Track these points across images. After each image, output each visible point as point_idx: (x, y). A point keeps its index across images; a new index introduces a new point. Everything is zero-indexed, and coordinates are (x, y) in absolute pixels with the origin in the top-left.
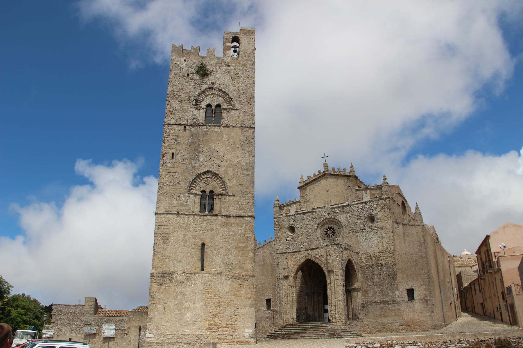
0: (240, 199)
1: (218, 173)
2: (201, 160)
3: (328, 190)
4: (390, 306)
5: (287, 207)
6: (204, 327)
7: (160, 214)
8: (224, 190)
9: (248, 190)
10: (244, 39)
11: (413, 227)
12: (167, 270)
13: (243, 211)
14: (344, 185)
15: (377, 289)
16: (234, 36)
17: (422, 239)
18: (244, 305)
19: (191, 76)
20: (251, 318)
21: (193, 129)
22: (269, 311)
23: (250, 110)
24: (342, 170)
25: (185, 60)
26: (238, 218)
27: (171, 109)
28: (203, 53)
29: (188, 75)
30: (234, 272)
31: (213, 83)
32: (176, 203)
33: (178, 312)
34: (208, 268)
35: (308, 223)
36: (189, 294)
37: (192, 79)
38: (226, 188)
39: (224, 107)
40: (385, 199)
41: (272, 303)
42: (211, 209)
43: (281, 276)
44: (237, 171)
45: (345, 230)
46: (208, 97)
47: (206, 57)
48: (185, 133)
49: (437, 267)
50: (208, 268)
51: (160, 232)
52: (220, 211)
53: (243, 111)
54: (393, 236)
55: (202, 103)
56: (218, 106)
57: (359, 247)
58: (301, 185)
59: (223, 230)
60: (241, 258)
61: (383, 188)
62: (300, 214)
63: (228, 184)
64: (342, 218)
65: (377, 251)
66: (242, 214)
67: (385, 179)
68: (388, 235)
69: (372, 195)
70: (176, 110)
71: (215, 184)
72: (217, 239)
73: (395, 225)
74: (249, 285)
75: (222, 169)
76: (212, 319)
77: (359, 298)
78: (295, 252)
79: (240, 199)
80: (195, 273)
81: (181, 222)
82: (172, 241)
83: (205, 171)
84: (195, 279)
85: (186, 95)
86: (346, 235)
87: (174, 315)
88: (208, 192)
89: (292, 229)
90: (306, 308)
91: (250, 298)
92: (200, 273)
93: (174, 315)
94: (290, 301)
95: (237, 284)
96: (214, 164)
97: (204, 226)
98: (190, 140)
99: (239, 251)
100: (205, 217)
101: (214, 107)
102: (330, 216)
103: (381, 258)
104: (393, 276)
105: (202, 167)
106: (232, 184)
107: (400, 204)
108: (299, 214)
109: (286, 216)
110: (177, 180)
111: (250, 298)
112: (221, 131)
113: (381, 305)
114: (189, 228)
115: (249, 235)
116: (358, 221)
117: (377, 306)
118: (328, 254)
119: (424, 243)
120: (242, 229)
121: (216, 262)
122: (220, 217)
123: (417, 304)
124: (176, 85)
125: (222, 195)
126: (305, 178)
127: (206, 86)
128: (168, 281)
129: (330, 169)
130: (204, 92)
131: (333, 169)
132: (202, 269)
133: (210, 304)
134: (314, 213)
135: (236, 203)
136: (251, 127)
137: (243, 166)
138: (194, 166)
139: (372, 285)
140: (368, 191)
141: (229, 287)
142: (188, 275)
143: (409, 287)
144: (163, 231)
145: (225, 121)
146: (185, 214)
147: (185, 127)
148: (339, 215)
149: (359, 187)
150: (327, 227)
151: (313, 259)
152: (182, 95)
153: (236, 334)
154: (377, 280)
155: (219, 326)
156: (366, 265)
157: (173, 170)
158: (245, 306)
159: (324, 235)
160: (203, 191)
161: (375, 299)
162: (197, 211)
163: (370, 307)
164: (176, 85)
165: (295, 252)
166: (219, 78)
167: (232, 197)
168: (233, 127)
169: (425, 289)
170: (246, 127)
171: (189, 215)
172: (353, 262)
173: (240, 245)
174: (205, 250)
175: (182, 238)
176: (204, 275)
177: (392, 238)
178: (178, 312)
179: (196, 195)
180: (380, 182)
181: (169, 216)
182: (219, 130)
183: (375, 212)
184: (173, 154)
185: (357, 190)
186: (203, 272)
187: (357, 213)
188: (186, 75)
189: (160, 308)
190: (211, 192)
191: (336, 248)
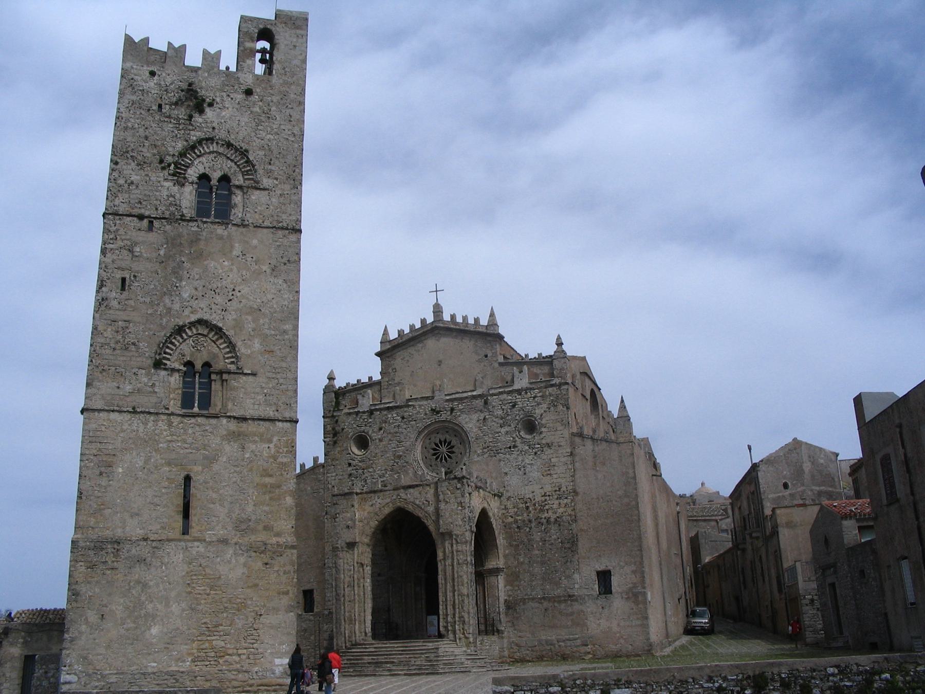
0: (267, 383)
1: (220, 325)
2: (185, 295)
3: (440, 362)
4: (563, 606)
5: (353, 394)
6: (189, 654)
7: (94, 410)
8: (232, 363)
9: (284, 365)
10: (283, 36)
11: (614, 446)
12: (108, 533)
13: (274, 408)
14: (477, 353)
15: (537, 569)
16: (261, 26)
17: (631, 471)
18: (274, 608)
19: (166, 108)
20: (289, 634)
21: (168, 227)
22: (309, 616)
23: (293, 191)
24: (471, 321)
25: (153, 74)
26: (262, 423)
27: (121, 181)
28: (193, 59)
29: (160, 106)
30: (253, 538)
31: (214, 128)
32: (128, 388)
33: (132, 625)
34: (198, 528)
35: (396, 430)
36: (157, 585)
37: (169, 117)
38: (237, 357)
39: (237, 183)
40: (560, 385)
41: (317, 597)
42: (206, 402)
43: (341, 543)
44: (261, 321)
45: (474, 447)
46: (203, 159)
47: (199, 68)
48: (150, 235)
49: (657, 525)
50: (198, 528)
51: (95, 452)
52: (224, 405)
53: (278, 192)
54: (573, 462)
55: (190, 171)
56: (225, 179)
57: (503, 482)
58: (385, 348)
59: (230, 449)
60: (266, 508)
61: (555, 362)
62: (380, 410)
63: (242, 350)
64: (470, 422)
65: (538, 494)
66: (272, 414)
67: (559, 344)
68: (563, 459)
69: (533, 375)
70: (132, 183)
71: (215, 350)
72: (216, 467)
73: (577, 440)
74: (284, 565)
75: (231, 317)
76: (204, 638)
77: (501, 587)
78: (371, 492)
79: (267, 383)
80: (169, 540)
81: (141, 430)
82: (120, 470)
83: (193, 319)
84: (169, 553)
85: (155, 151)
86: (476, 458)
87: (122, 632)
88: (198, 366)
89: (363, 442)
90: (389, 610)
91: (287, 593)
92: (180, 540)
93: (122, 632)
94: (359, 596)
95: (260, 564)
96: (213, 306)
97: (190, 440)
98: (162, 252)
99: (264, 493)
100: (193, 420)
101: (214, 182)
103: (547, 507)
104: (571, 545)
105: (187, 312)
106: (250, 349)
107: (588, 397)
108: (376, 410)
109: (350, 414)
110: (131, 338)
111: (287, 593)
112: (229, 236)
113: (546, 604)
114: (158, 442)
115: (285, 460)
116: (503, 430)
117: (537, 605)
118: (441, 497)
119: (635, 478)
120: (272, 446)
121: (214, 516)
122: (224, 421)
123: (618, 603)
124: (133, 128)
125: (229, 373)
126: (393, 335)
127: (198, 134)
128: (110, 558)
129: (447, 317)
130: (193, 148)
131: (453, 317)
132: (185, 531)
133: (200, 607)
135: (258, 390)
136: (293, 229)
137: (275, 312)
138: (170, 309)
139: (527, 561)
140: (525, 368)
141: (240, 571)
142: (154, 544)
143: (601, 568)
144: (100, 450)
145: (237, 214)
146: (149, 413)
147: (151, 223)
148: (464, 416)
149: (505, 358)
150: (436, 438)
151: (410, 508)
152: (145, 150)
153: (256, 669)
154: (537, 552)
155: (221, 654)
156: (516, 521)
157: (122, 315)
158: (276, 610)
159: (429, 456)
160: (189, 364)
161: (532, 590)
162: (175, 405)
163: (523, 607)
164: (133, 128)
165: (371, 492)
166: (225, 117)
167: (251, 378)
168: (256, 227)
169: (634, 572)
170: (282, 228)
171: (157, 414)
172: (491, 514)
173: (267, 480)
174: (193, 491)
175: (141, 464)
176: (190, 544)
177: (570, 467)
178: (132, 625)
179: (173, 370)
180: (549, 350)
181: (114, 416)
182: (226, 233)
183: (538, 411)
184: (124, 280)
185: (501, 364)
186: (186, 537)
187: (500, 412)
188: (155, 108)
189: (93, 617)
190: (207, 365)
191: (459, 486)
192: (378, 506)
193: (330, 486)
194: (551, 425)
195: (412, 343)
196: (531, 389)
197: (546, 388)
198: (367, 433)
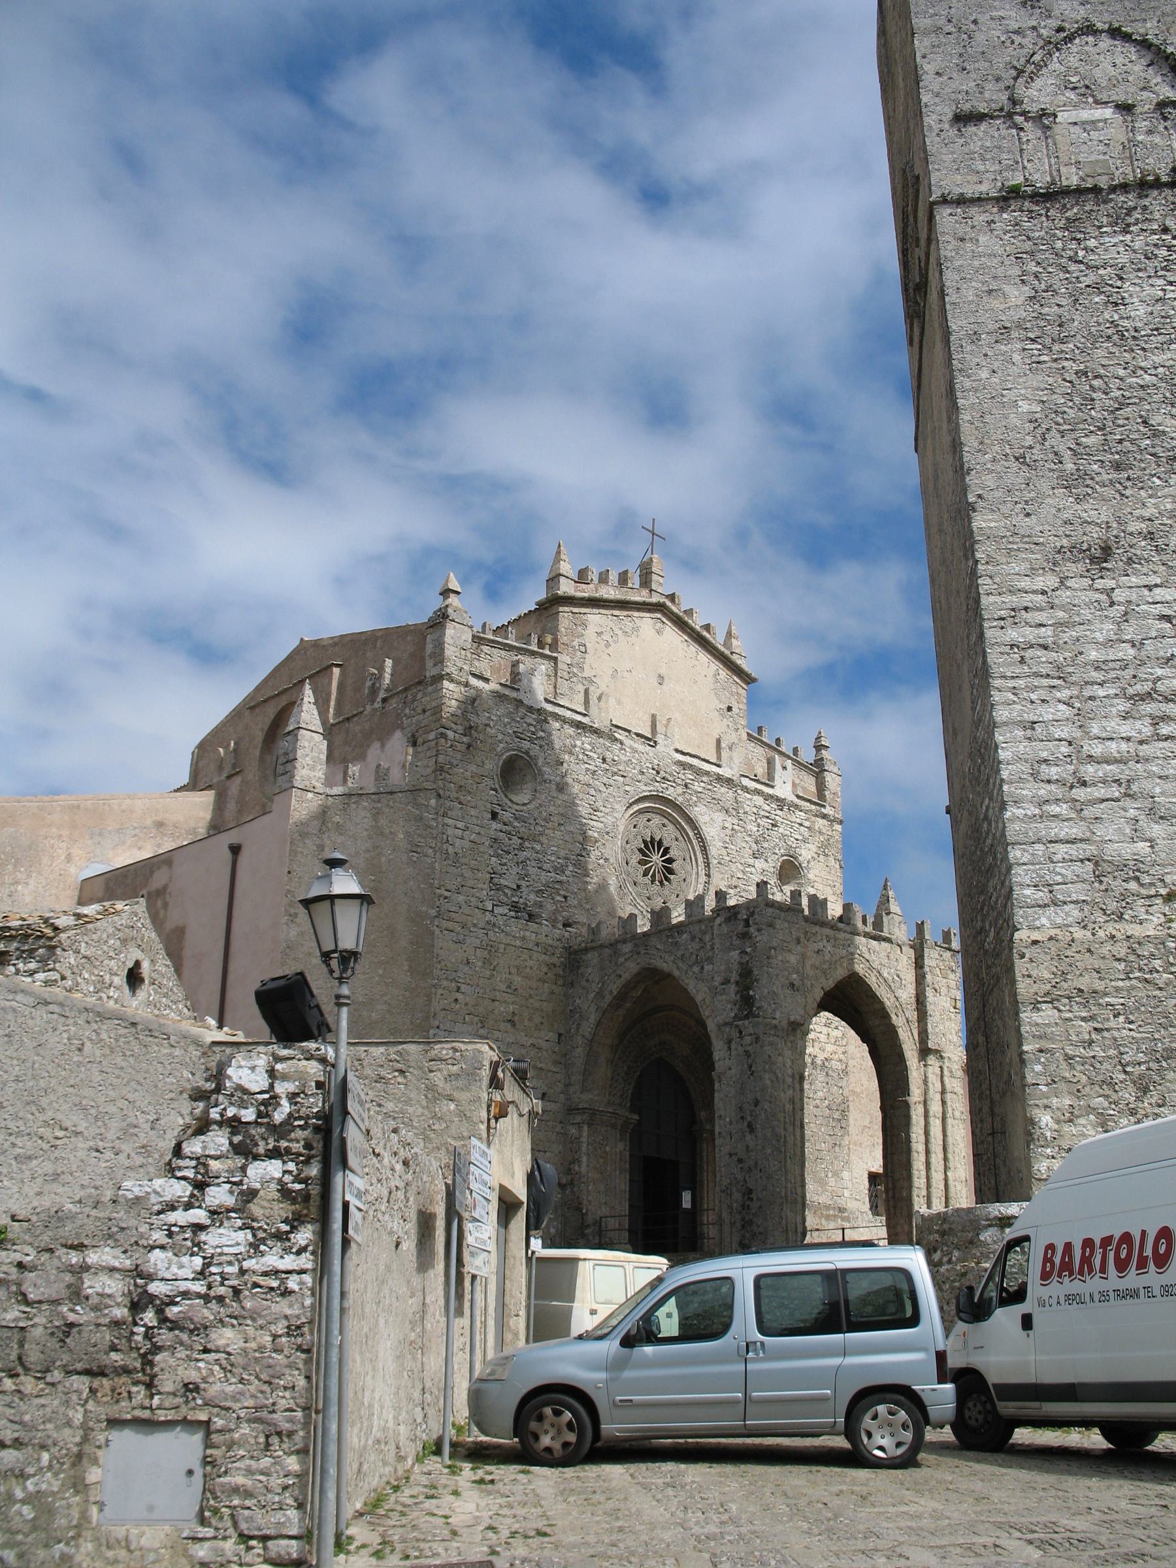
40: (832, 821)
102: (671, 793)
151: (872, 981)
195: (616, 612)
196: (796, 806)
197: (816, 816)
198: (536, 758)
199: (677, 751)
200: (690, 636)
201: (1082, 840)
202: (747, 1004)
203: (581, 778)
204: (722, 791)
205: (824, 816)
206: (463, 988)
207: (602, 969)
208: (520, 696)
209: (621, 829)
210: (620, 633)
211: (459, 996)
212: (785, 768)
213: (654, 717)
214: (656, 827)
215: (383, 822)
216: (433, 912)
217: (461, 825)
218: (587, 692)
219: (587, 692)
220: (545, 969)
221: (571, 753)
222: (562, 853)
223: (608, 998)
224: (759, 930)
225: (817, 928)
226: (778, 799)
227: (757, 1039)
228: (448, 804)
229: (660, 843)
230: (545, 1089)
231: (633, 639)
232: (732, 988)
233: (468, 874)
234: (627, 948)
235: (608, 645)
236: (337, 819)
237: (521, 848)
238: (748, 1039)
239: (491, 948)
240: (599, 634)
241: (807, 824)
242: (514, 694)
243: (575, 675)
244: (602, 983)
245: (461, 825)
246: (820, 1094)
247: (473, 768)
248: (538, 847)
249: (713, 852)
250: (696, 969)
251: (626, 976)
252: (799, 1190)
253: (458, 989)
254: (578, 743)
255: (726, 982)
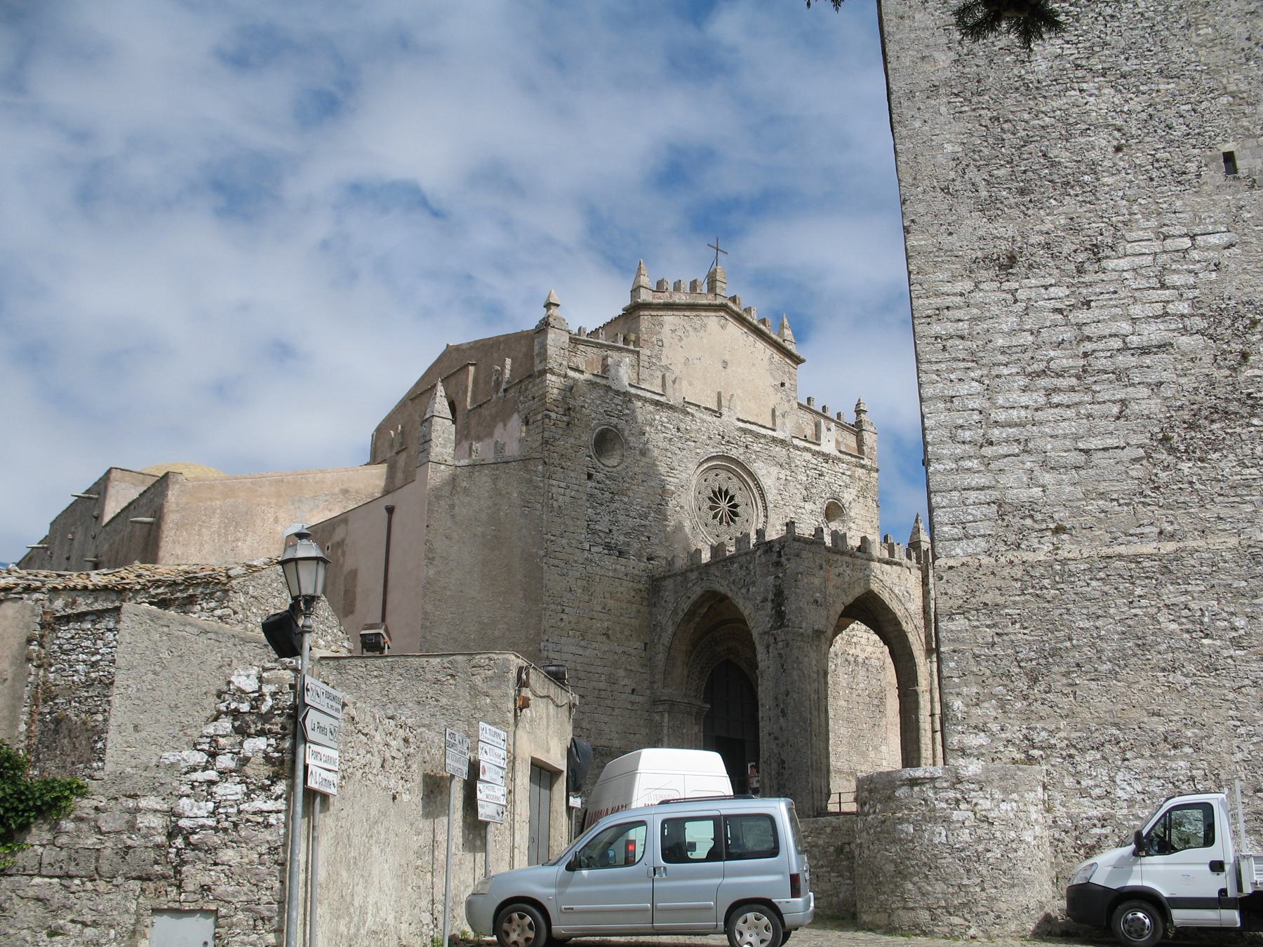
40: (870, 470)
102: (734, 453)
134: (689, 418)
151: (885, 596)
192: (847, 579)
193: (555, 504)
194: (860, 523)
195: (687, 313)
196: (839, 459)
199: (739, 420)
200: (749, 329)
201: (989, 488)
202: (780, 617)
203: (660, 444)
204: (777, 450)
205: (863, 466)
206: (567, 610)
207: (676, 592)
208: (609, 383)
209: (694, 482)
210: (690, 329)
211: (564, 616)
212: (829, 429)
213: (719, 393)
214: (723, 480)
215: (500, 484)
216: (542, 553)
217: (563, 485)
218: (663, 377)
219: (663, 377)
220: (633, 594)
221: (651, 425)
222: (646, 503)
223: (681, 615)
224: (788, 560)
225: (838, 556)
226: (824, 454)
227: (787, 645)
228: (552, 469)
229: (727, 492)
230: (634, 686)
231: (702, 333)
232: (769, 605)
233: (569, 522)
234: (693, 576)
235: (681, 339)
236: (465, 484)
237: (612, 500)
238: (780, 644)
239: (589, 578)
240: (673, 331)
241: (848, 473)
242: (604, 382)
243: (654, 364)
244: (676, 602)
245: (563, 485)
246: (862, 685)
247: (572, 440)
248: (626, 499)
249: (771, 497)
250: (744, 591)
251: (694, 597)
252: (824, 761)
253: (563, 611)
254: (657, 417)
255: (765, 600)
